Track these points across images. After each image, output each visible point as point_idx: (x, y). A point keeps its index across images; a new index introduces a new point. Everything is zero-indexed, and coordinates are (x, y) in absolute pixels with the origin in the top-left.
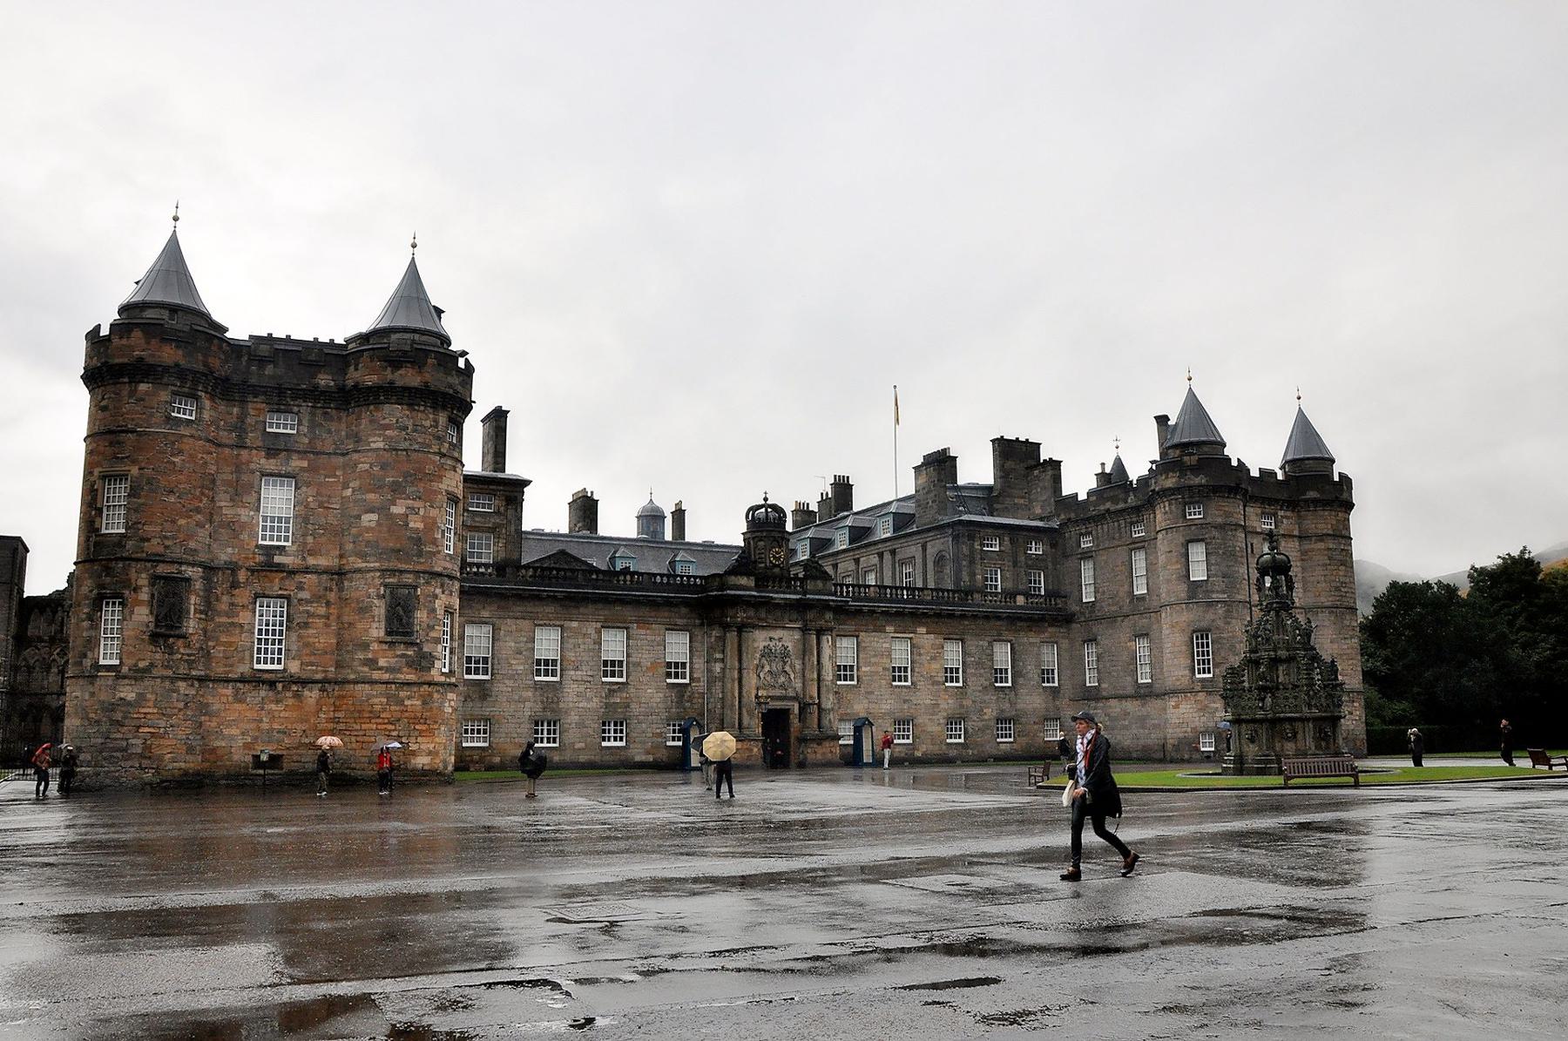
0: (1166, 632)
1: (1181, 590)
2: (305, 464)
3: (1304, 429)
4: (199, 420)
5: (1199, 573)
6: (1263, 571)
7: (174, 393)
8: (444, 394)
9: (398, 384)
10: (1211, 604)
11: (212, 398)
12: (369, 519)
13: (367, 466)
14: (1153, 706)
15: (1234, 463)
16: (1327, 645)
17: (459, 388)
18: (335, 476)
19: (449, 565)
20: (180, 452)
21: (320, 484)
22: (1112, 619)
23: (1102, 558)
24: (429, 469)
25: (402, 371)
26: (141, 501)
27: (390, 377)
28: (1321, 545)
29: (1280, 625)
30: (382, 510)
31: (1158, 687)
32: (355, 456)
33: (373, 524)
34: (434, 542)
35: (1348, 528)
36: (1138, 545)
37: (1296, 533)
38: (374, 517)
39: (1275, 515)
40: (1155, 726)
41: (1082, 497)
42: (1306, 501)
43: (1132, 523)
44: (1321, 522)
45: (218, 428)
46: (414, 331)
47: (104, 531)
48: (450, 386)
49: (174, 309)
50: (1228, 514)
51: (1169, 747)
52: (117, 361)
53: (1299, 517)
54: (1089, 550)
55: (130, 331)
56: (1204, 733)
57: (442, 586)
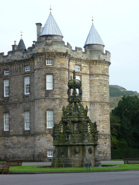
0: (36, 110)
1: (43, 94)
3: (92, 31)
5: (49, 87)
6: (70, 87)
10: (54, 100)
14: (30, 139)
15: (66, 44)
16: (98, 117)
22: (15, 105)
23: (13, 79)
28: (97, 78)
29: (76, 109)
31: (32, 132)
35: (108, 72)
36: (26, 74)
37: (88, 73)
39: (80, 66)
40: (31, 147)
41: (6, 54)
42: (93, 61)
43: (25, 66)
44: (99, 69)
50: (62, 64)
51: (36, 156)
53: (90, 67)
54: (7, 76)
56: (49, 150)
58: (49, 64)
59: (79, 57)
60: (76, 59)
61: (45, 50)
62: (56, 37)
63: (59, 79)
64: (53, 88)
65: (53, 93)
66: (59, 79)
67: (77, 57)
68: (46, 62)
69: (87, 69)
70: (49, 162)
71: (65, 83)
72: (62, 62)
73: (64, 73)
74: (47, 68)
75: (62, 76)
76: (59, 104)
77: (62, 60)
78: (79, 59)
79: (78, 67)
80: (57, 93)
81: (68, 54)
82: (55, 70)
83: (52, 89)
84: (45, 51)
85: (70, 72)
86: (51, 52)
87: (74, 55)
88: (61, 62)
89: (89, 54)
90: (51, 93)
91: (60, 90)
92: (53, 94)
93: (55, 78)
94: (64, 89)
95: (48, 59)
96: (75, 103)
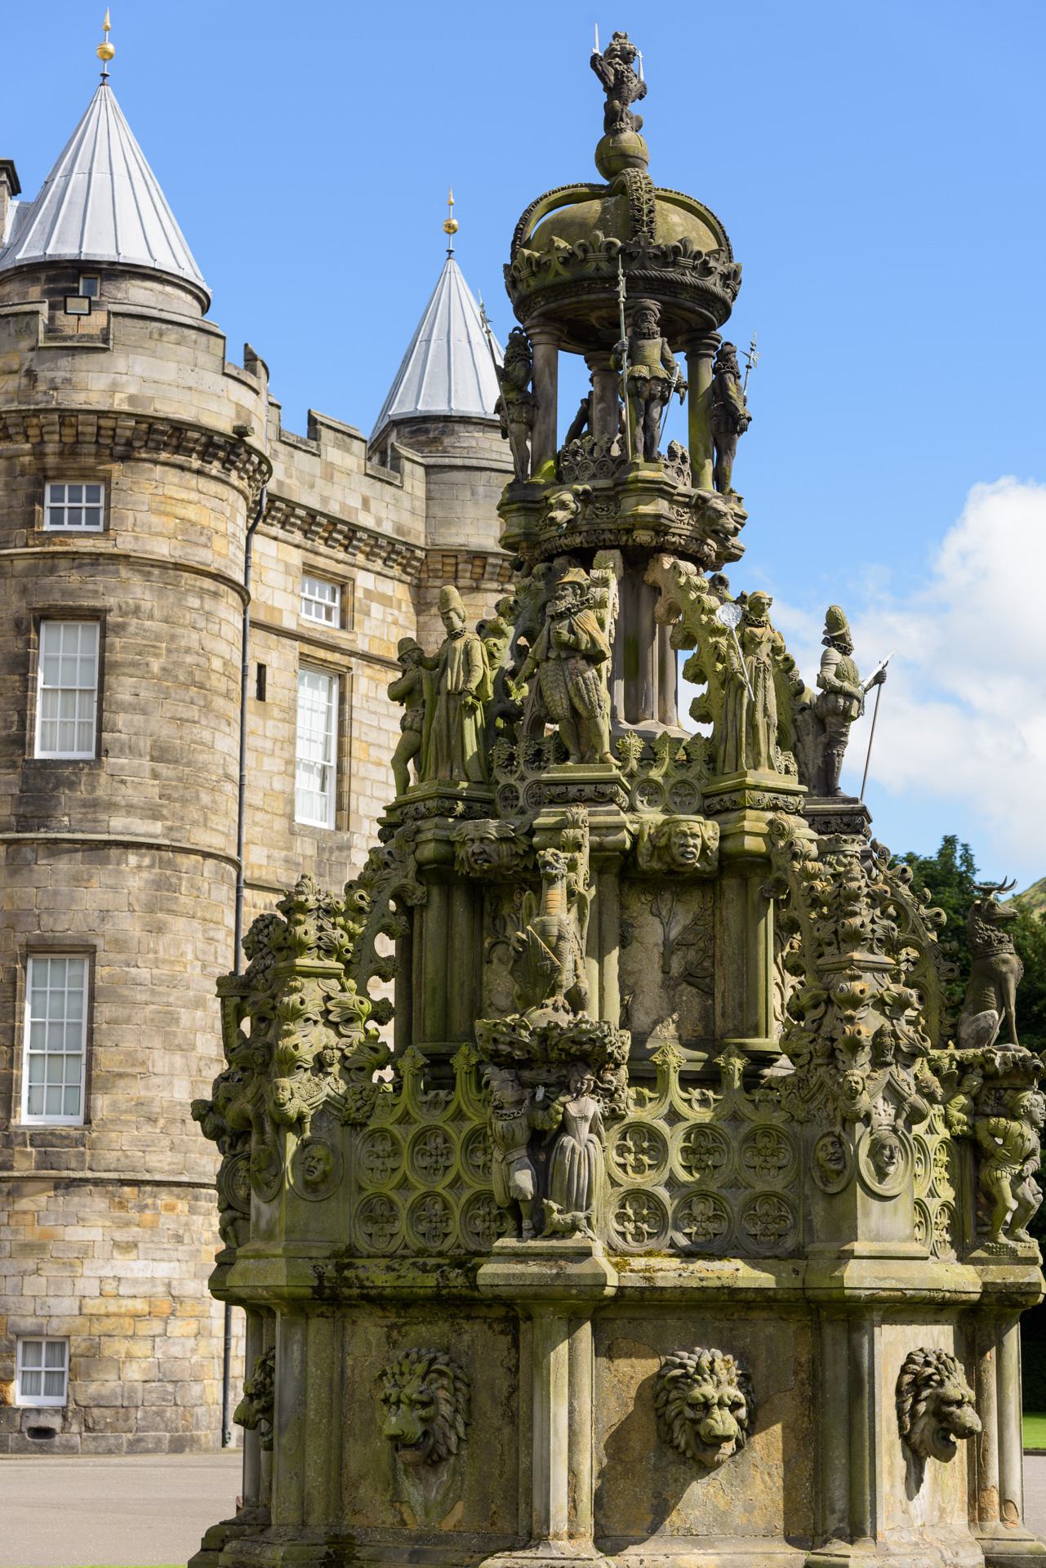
39: (343, 585)
58: (74, 520)
59: (334, 509)
60: (312, 514)
61: (41, 387)
62: (149, 284)
63: (156, 666)
64: (101, 751)
65: (100, 793)
66: (156, 666)
67: (325, 500)
68: (48, 502)
69: (395, 623)
70: (21, 1450)
71: (207, 708)
72: (191, 513)
73: (208, 615)
74: (54, 555)
75: (192, 639)
76: (143, 897)
77: (194, 496)
78: (334, 521)
79: (324, 595)
80: (128, 794)
81: (251, 450)
82: (125, 585)
83: (91, 755)
84: (40, 399)
85: (256, 624)
86: (101, 414)
87: (292, 482)
88: (181, 512)
89: (420, 490)
90: (82, 792)
91: (161, 768)
92: (94, 805)
93: (119, 657)
94: (204, 768)
95: (61, 474)
96: (637, 562)
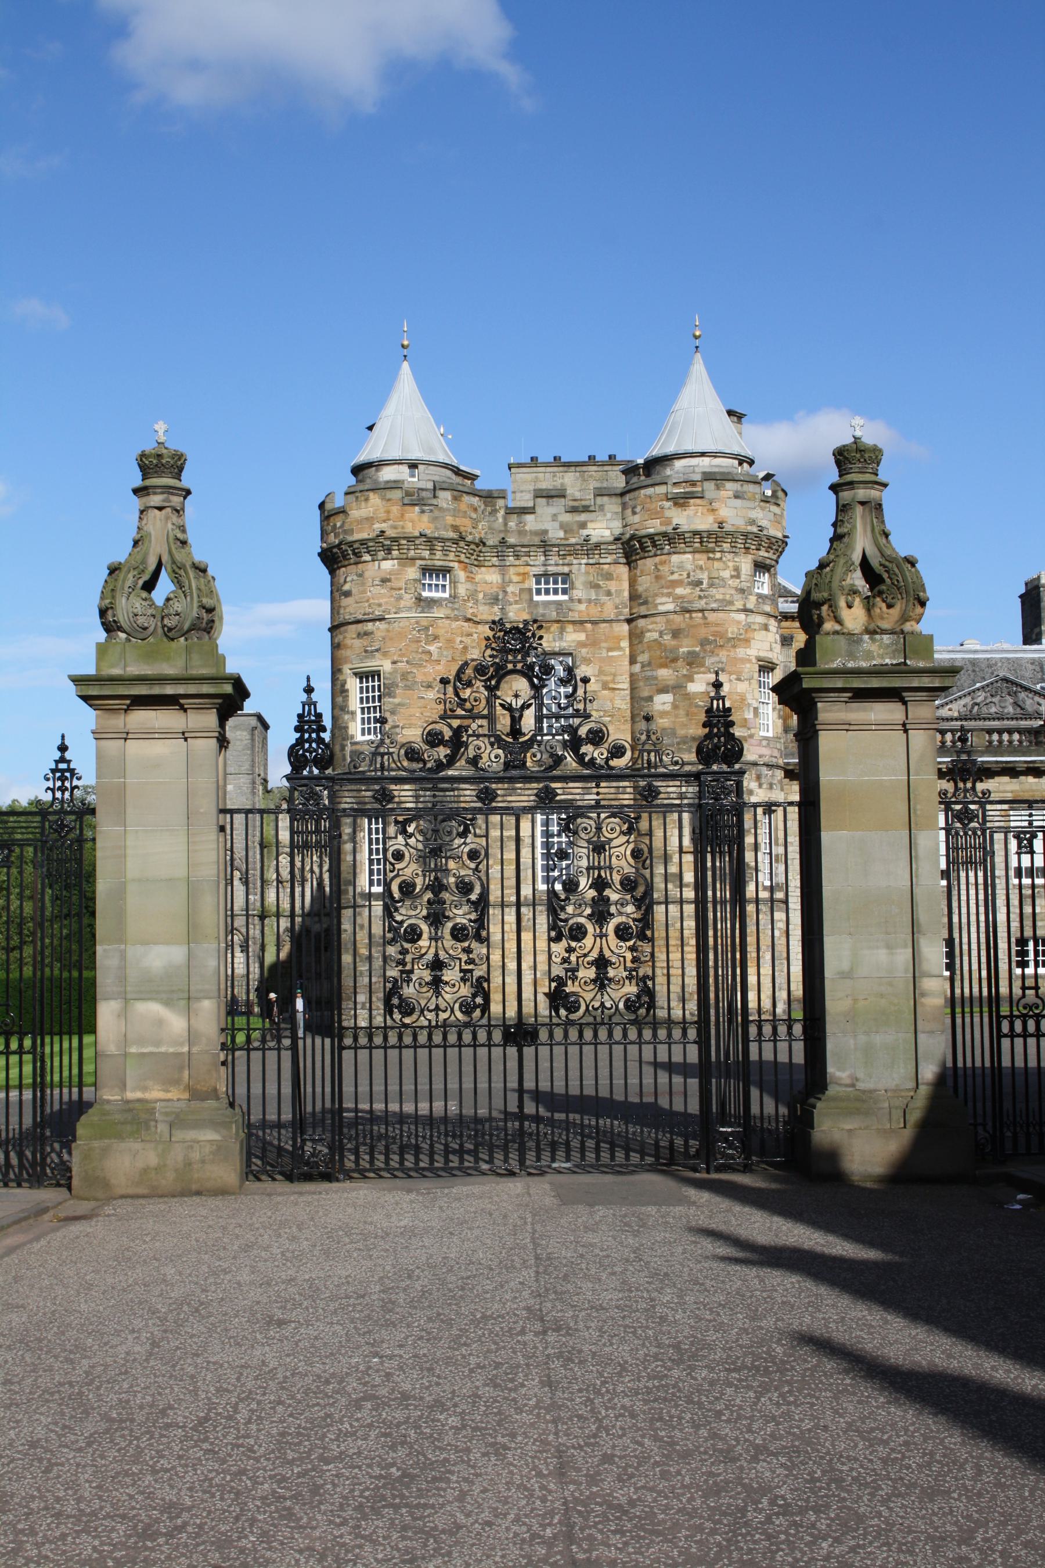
2: (582, 637)
4: (454, 597)
7: (426, 571)
8: (746, 535)
9: (685, 528)
11: (465, 567)
12: (662, 702)
13: (655, 635)
17: (764, 523)
18: (620, 649)
19: (766, 752)
20: (436, 638)
21: (602, 660)
24: (732, 631)
25: (690, 511)
26: (397, 700)
27: (675, 521)
30: (677, 688)
32: (641, 623)
33: (668, 707)
34: (745, 723)
38: (668, 698)
45: (476, 602)
46: (703, 454)
47: (359, 738)
48: (752, 522)
49: (413, 466)
52: (357, 536)
55: (367, 500)
57: (759, 777)
